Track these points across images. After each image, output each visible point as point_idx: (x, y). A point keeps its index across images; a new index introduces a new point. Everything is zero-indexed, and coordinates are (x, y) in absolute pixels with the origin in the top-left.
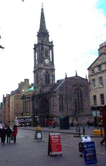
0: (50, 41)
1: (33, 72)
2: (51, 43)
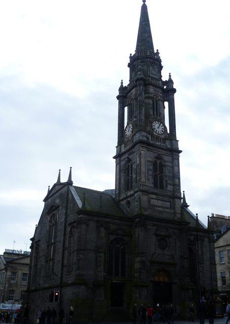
0: (165, 78)
1: (114, 158)
2: (166, 83)
